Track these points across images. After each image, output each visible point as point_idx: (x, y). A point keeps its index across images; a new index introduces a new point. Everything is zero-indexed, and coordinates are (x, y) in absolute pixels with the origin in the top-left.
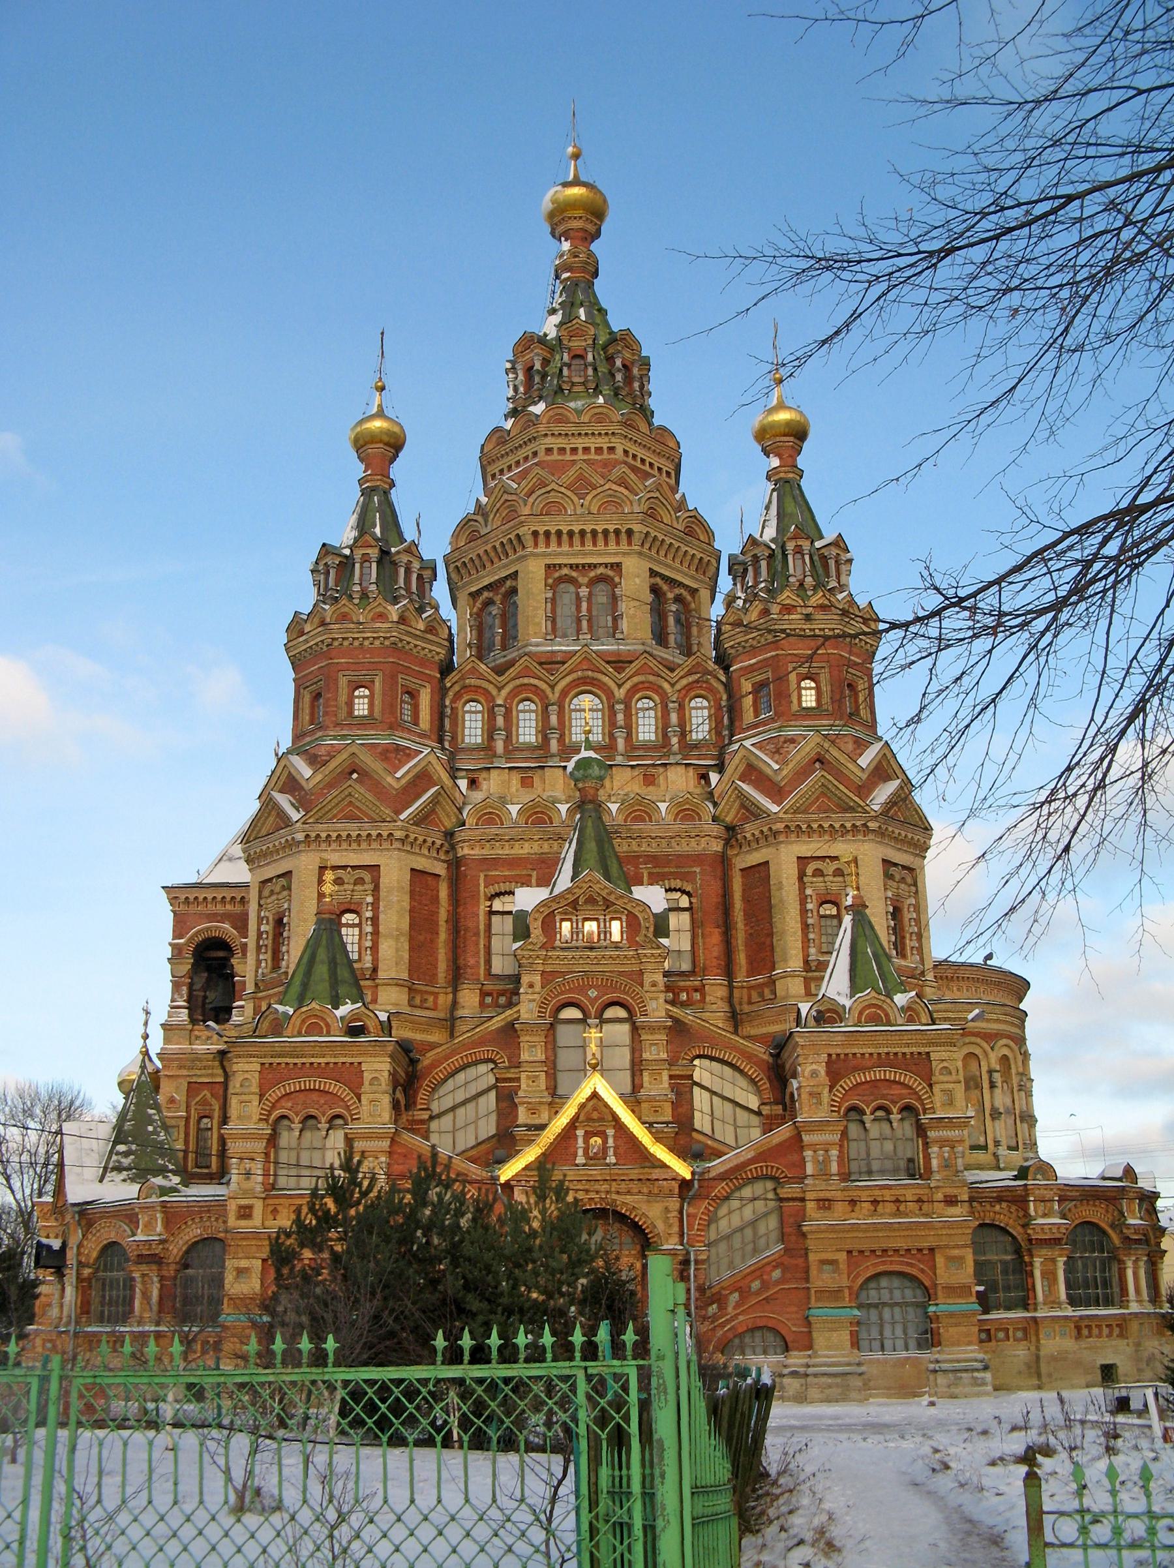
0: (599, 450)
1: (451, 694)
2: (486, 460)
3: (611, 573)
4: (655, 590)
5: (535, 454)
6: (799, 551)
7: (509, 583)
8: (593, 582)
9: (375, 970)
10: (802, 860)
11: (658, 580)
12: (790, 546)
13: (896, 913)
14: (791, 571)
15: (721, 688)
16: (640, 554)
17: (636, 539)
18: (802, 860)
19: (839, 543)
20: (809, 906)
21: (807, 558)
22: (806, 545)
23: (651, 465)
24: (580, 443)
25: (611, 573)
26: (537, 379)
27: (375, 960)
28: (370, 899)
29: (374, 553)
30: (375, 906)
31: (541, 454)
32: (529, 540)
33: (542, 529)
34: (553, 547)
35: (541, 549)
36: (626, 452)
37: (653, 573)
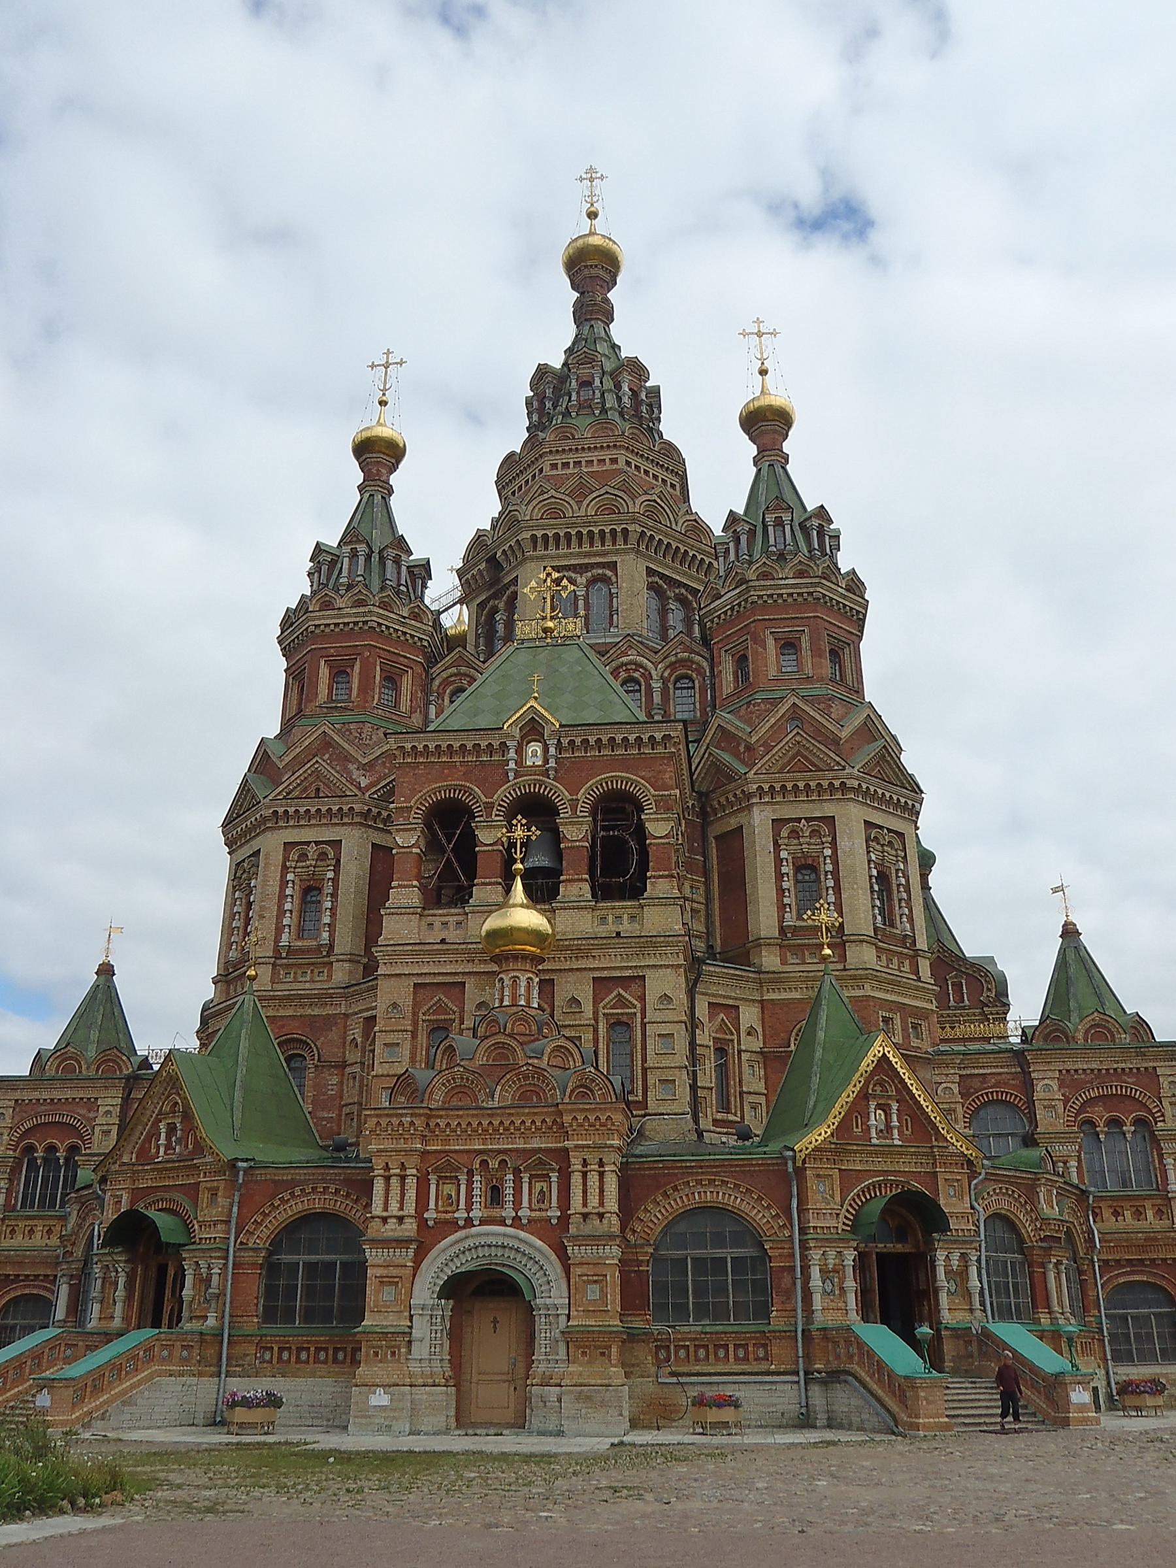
0: (602, 461)
1: (437, 682)
2: (503, 483)
3: (609, 573)
4: (651, 587)
5: (541, 471)
6: (779, 523)
7: (512, 588)
8: (592, 582)
9: (331, 947)
10: (778, 823)
11: (657, 579)
12: (770, 518)
13: (883, 878)
14: (772, 541)
15: (705, 664)
16: (638, 552)
17: (633, 538)
18: (778, 823)
19: (821, 511)
20: (784, 870)
21: (788, 528)
22: (786, 517)
23: (655, 477)
24: (585, 457)
25: (609, 573)
26: (548, 405)
27: (332, 936)
28: (330, 875)
29: (362, 548)
30: (335, 880)
31: (546, 468)
32: (527, 546)
33: (539, 534)
34: (552, 551)
35: (541, 552)
36: (628, 463)
37: (650, 572)
